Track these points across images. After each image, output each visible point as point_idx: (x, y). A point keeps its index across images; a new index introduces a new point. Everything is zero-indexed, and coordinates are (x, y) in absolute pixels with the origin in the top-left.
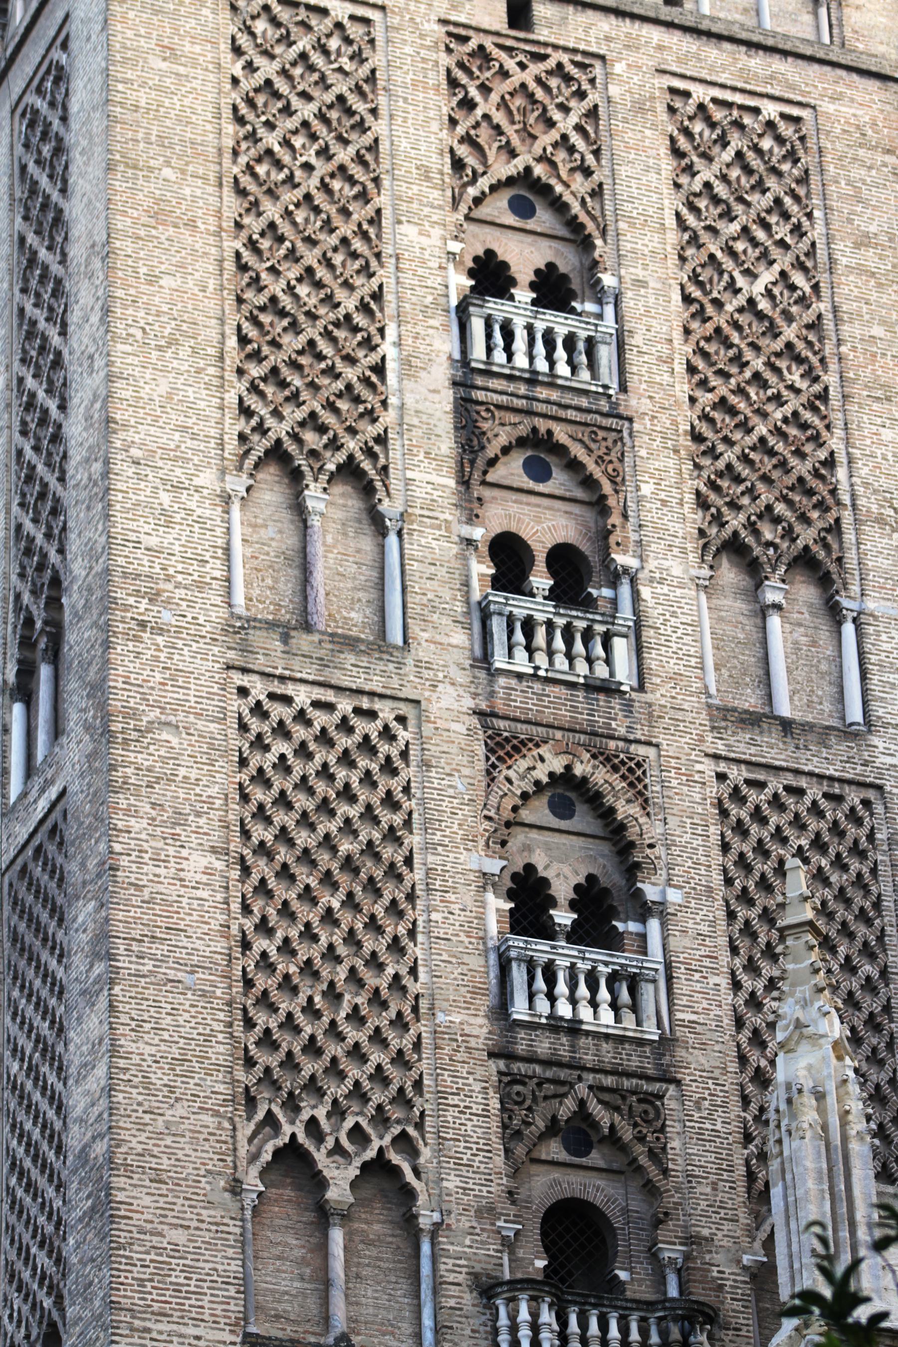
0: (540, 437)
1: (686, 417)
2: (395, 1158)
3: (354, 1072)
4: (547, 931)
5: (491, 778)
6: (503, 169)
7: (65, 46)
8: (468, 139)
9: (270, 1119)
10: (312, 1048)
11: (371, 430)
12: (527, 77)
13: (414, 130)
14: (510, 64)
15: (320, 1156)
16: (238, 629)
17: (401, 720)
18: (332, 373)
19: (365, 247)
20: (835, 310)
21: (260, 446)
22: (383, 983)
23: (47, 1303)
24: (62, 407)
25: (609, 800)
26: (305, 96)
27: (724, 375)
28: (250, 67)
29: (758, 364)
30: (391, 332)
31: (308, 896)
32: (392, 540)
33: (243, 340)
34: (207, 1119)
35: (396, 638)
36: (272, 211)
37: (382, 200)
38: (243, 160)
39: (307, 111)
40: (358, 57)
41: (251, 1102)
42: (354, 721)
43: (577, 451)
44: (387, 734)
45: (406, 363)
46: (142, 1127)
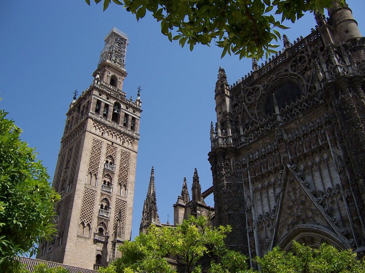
0: (108, 174)
1: (118, 174)
2: (90, 223)
3: (88, 217)
4: (103, 209)
5: (101, 197)
6: (109, 154)
7: (81, 140)
8: (107, 152)
9: (82, 219)
10: (85, 215)
11: (97, 172)
12: (112, 148)
13: (104, 151)
14: (111, 147)
15: (85, 222)
16: (86, 184)
18: (95, 167)
21: (89, 172)
22: (91, 211)
23: (63, 230)
24: (76, 166)
26: (97, 147)
27: (121, 171)
28: (94, 145)
29: (124, 171)
31: (87, 204)
33: (90, 164)
35: (96, 186)
36: (93, 155)
37: (101, 155)
39: (97, 148)
40: (101, 145)
41: (81, 218)
43: (111, 175)
44: (94, 193)
45: (100, 167)
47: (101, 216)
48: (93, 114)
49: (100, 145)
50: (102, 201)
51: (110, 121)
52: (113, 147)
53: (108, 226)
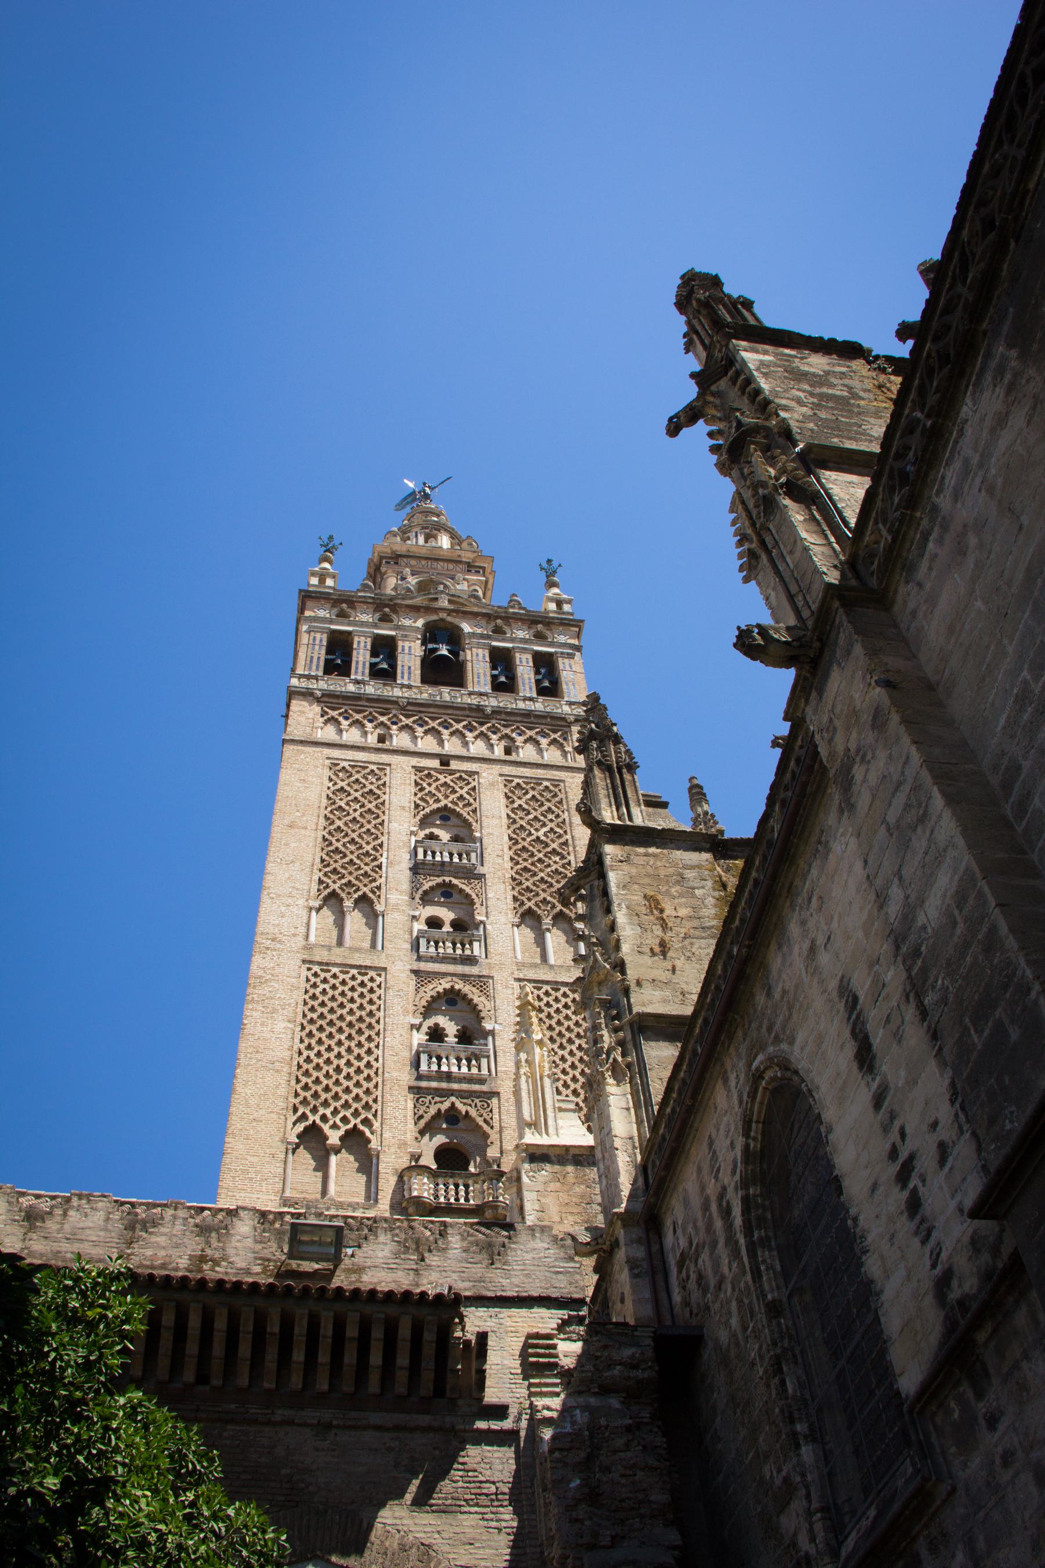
2: (361, 1127)
5: (417, 991)
6: (435, 806)
8: (422, 799)
12: (448, 780)
14: (439, 776)
15: (326, 1128)
16: (308, 948)
17: (380, 975)
19: (376, 832)
20: (573, 837)
25: (470, 996)
30: (385, 855)
32: (380, 918)
34: (274, 1116)
38: (329, 809)
41: (295, 1109)
42: (357, 976)
46: (242, 1119)
47: (429, 1078)
48: (316, 678)
49: (374, 780)
50: (428, 1011)
51: (409, 687)
52: (452, 773)
53: (496, 1125)
